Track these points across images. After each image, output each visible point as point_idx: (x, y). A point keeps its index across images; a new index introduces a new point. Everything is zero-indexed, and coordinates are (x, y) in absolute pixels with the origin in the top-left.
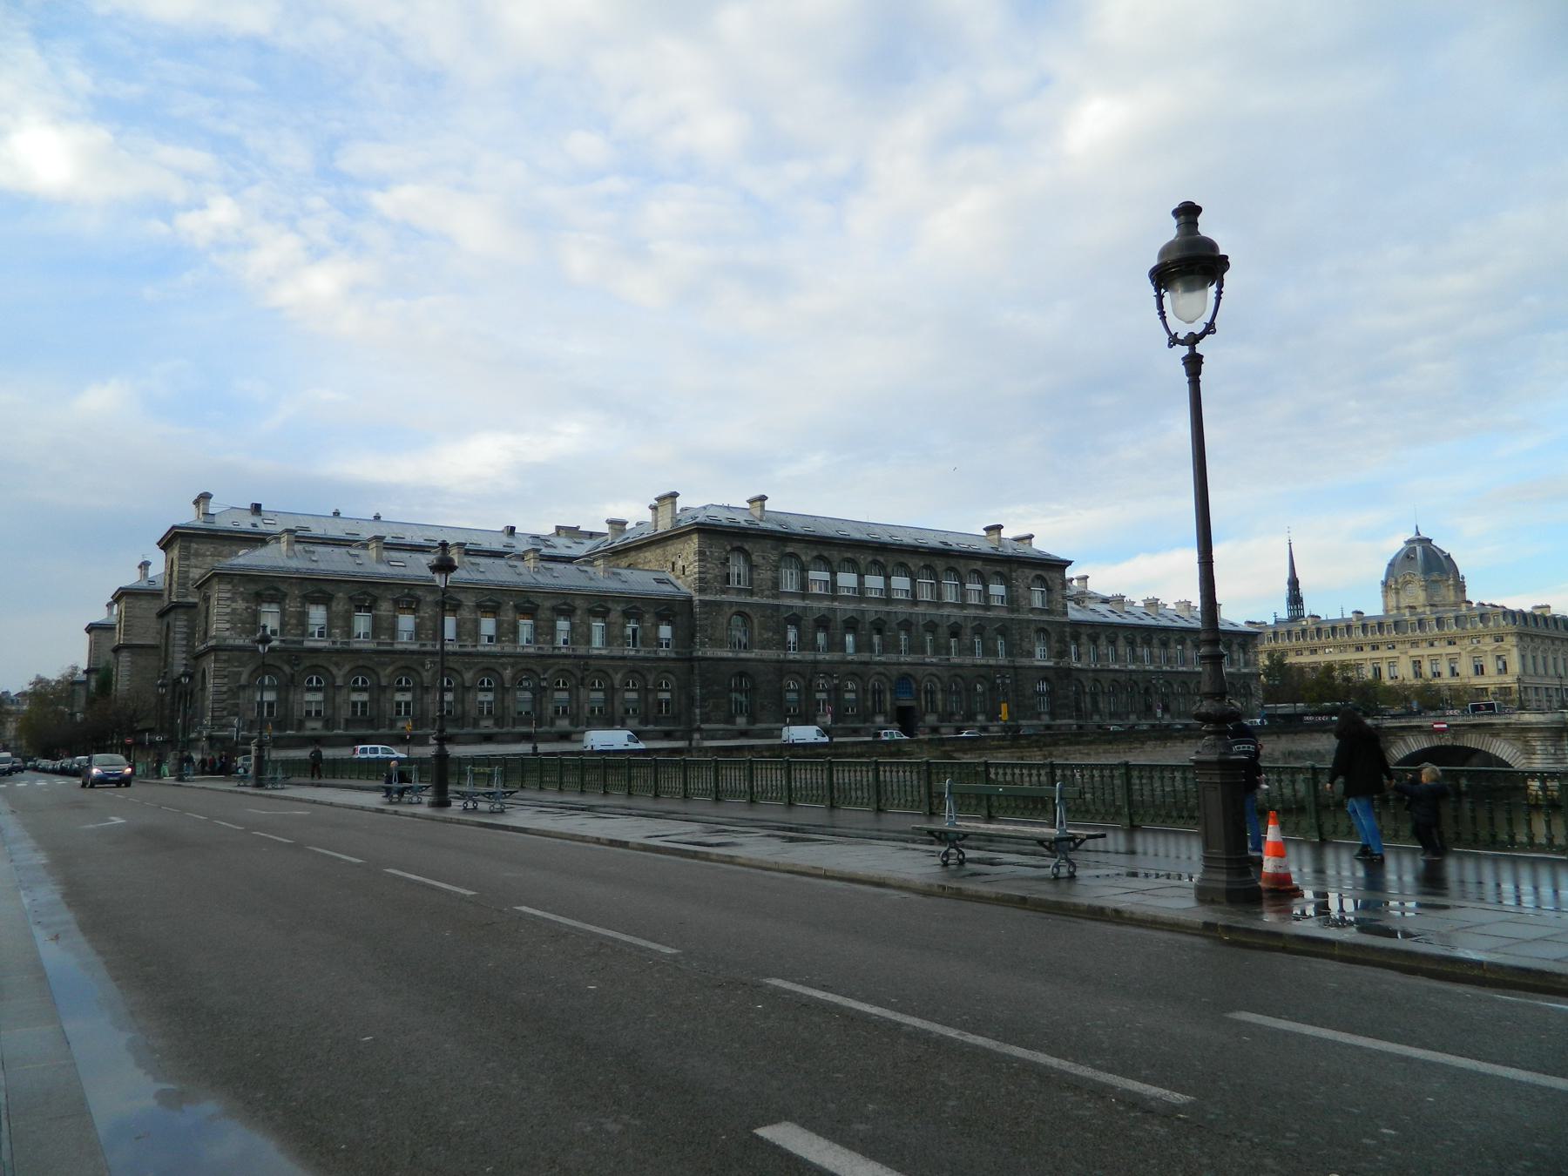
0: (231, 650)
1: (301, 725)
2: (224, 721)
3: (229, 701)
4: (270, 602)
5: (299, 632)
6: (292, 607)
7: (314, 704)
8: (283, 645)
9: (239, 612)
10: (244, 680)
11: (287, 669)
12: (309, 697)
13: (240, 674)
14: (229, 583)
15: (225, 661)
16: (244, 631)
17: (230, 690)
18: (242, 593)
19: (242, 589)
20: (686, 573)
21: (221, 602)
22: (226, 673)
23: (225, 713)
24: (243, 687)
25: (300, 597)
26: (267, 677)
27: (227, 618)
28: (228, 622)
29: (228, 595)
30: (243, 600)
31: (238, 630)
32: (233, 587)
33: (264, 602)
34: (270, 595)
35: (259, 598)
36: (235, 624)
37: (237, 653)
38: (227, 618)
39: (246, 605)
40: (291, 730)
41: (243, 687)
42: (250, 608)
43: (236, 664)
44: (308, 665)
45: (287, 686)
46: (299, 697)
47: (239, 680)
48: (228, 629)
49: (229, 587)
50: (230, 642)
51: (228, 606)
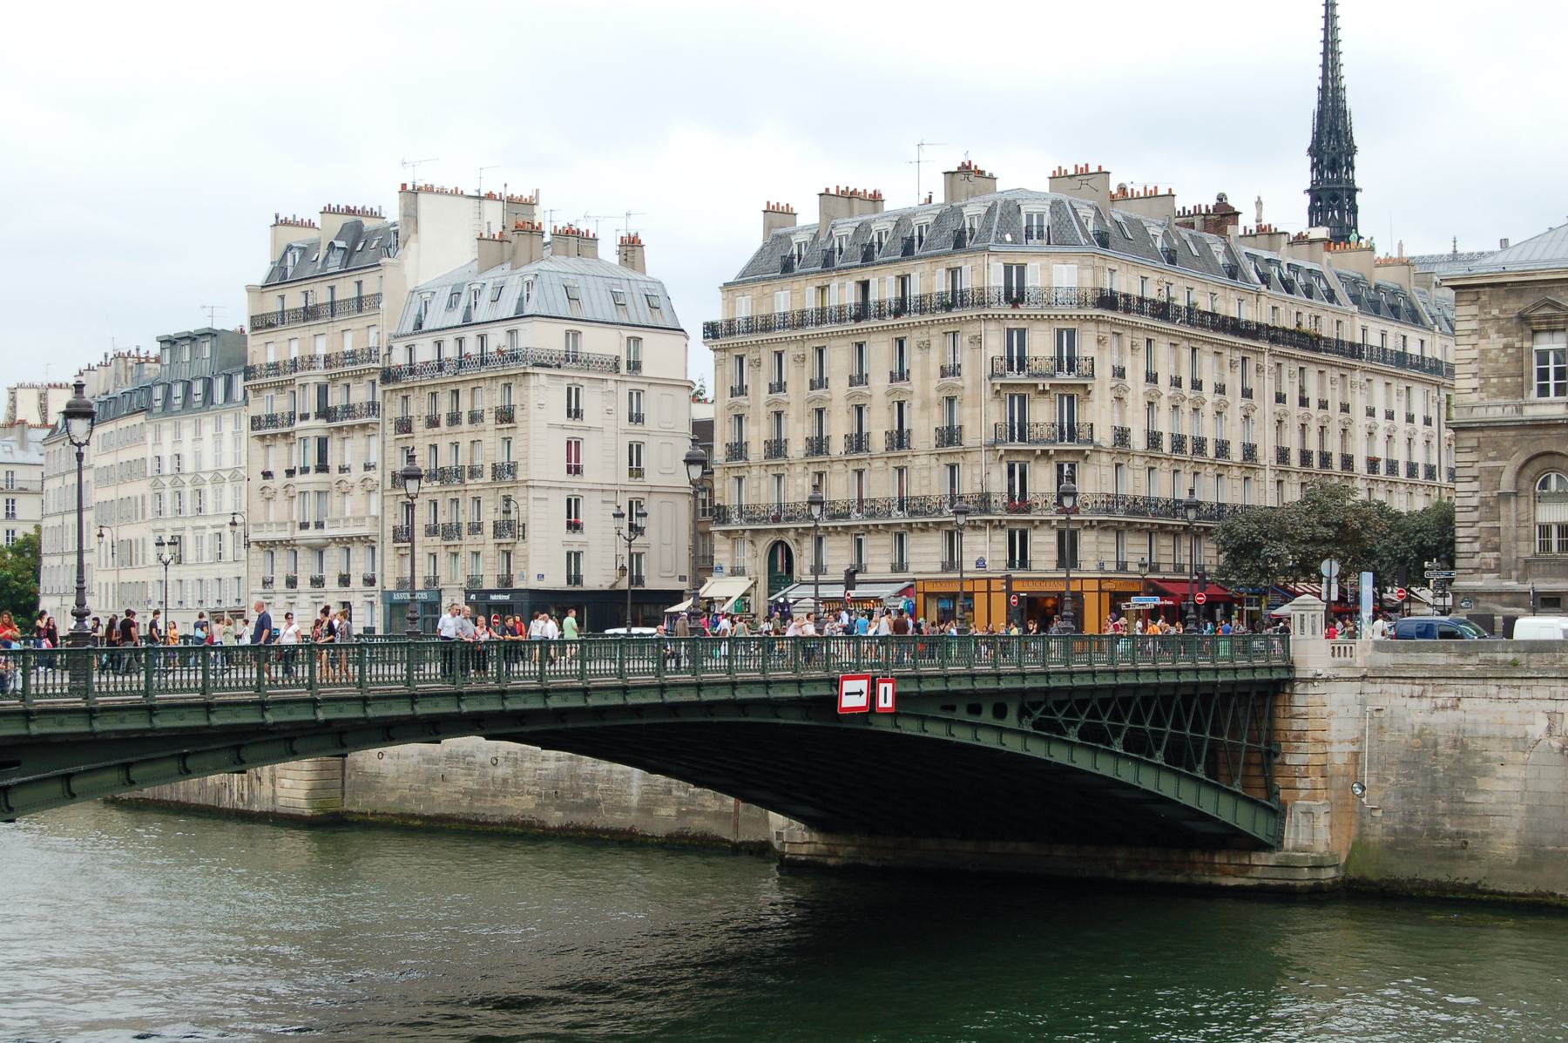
0: (1481, 429)
3: (1481, 524)
9: (1492, 355)
10: (1507, 484)
13: (1499, 472)
14: (1473, 302)
15: (1473, 449)
16: (1502, 392)
18: (1497, 319)
19: (1495, 312)
23: (1477, 546)
24: (1505, 497)
26: (1553, 477)
27: (1474, 368)
28: (1475, 375)
29: (1474, 325)
30: (1498, 332)
31: (1493, 390)
32: (1482, 307)
33: (1535, 332)
34: (1545, 317)
35: (1527, 324)
37: (1494, 434)
38: (1474, 368)
39: (1505, 340)
41: (1505, 497)
42: (1512, 346)
43: (1492, 454)
47: (1497, 487)
48: (1475, 389)
49: (1474, 310)
50: (1480, 415)
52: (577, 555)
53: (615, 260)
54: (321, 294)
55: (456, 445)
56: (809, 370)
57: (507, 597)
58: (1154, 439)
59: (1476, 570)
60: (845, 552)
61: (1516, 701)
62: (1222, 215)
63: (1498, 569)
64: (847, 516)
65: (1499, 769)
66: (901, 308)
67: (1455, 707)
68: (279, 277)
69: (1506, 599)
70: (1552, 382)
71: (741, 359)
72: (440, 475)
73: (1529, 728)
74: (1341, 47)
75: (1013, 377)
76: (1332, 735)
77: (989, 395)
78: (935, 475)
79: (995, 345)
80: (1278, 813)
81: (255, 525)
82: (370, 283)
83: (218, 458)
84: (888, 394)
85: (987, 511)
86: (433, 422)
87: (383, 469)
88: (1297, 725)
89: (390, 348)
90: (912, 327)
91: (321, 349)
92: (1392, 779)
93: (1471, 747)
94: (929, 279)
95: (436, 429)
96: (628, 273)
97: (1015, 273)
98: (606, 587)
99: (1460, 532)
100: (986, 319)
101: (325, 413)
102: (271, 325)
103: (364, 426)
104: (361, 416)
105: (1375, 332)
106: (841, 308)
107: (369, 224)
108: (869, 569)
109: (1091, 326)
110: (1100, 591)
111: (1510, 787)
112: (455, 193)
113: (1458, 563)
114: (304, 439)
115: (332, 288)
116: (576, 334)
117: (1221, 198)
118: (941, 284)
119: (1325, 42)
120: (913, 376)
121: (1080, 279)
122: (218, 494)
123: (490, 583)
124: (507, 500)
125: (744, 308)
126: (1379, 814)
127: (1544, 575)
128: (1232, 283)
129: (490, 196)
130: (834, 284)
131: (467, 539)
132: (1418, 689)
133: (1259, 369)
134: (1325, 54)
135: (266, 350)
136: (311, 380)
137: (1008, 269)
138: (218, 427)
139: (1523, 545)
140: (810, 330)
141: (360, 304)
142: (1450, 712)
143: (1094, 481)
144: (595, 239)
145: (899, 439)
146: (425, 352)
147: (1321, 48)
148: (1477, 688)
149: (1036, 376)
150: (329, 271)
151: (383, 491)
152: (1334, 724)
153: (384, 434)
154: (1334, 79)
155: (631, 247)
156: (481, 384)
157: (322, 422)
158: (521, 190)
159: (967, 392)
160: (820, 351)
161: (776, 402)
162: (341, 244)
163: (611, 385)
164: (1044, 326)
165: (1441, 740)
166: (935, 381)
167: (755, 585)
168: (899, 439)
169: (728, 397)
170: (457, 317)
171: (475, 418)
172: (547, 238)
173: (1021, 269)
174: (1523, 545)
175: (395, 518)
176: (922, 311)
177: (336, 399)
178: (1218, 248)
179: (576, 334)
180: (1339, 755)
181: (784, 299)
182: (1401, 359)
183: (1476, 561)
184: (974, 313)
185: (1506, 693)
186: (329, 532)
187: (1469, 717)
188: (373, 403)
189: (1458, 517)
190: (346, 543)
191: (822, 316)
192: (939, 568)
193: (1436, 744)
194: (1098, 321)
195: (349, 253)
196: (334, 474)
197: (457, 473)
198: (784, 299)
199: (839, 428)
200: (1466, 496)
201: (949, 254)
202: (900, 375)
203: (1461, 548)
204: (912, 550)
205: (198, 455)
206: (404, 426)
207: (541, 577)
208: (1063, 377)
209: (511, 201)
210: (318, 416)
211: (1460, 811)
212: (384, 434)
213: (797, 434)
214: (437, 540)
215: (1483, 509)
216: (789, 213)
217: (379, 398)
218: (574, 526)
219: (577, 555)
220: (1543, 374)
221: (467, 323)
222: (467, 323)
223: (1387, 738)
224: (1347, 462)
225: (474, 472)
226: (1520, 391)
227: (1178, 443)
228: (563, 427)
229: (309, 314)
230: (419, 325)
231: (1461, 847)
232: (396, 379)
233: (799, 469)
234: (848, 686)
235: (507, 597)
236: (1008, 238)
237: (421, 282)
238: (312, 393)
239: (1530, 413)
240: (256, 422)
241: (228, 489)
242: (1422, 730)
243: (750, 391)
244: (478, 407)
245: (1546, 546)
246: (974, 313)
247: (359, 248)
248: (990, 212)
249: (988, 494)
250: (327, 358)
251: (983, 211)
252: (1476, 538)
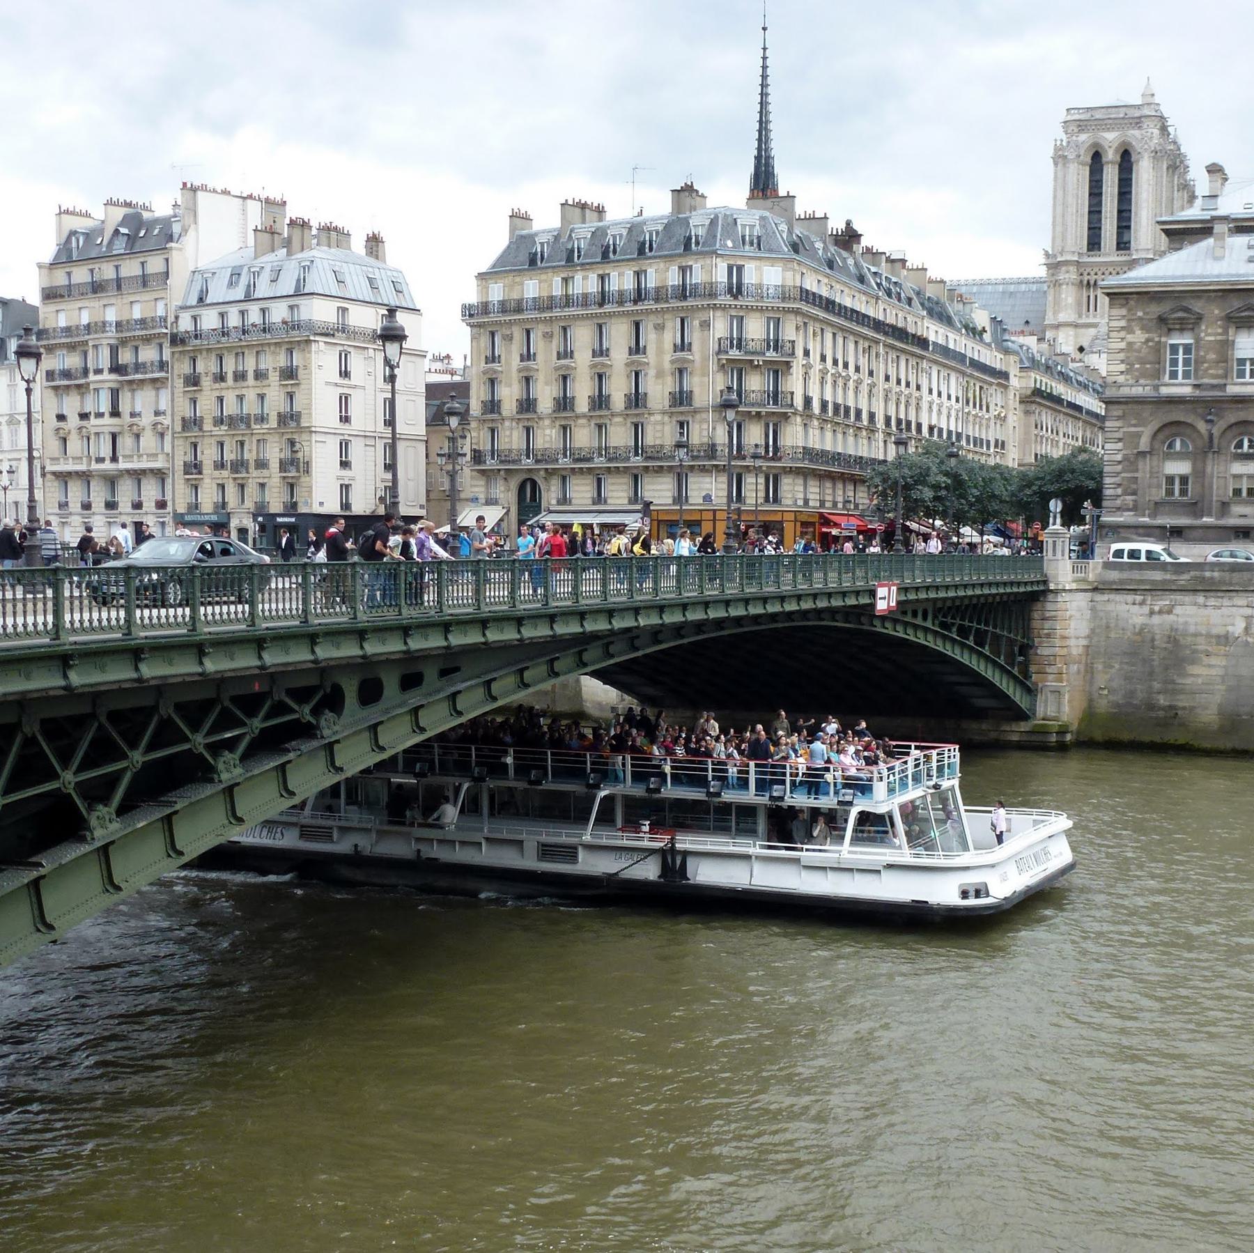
0: (1126, 403)
1: (1224, 507)
2: (1118, 502)
4: (1182, 330)
5: (1220, 372)
6: (1210, 333)
7: (1245, 479)
8: (1197, 393)
9: (1137, 346)
10: (1144, 444)
11: (1202, 426)
12: (1238, 468)
14: (1123, 306)
15: (1119, 418)
16: (1144, 375)
17: (1126, 458)
18: (1141, 319)
19: (1140, 314)
21: (1112, 335)
22: (1117, 435)
23: (1119, 491)
25: (1221, 319)
27: (1122, 356)
28: (1122, 362)
29: (1123, 323)
32: (1129, 310)
33: (1170, 330)
34: (1179, 319)
35: (1165, 324)
36: (1132, 365)
38: (1122, 356)
40: (1210, 515)
43: (1133, 422)
44: (1233, 420)
45: (1207, 449)
46: (1222, 468)
48: (1122, 373)
49: (1124, 312)
50: (1125, 391)
51: (1123, 339)
52: (347, 486)
53: (363, 252)
54: (107, 271)
55: (241, 398)
56: (556, 344)
57: (293, 520)
58: (824, 405)
59: (1119, 509)
60: (588, 488)
61: (1219, 608)
62: (849, 238)
63: (1135, 508)
64: (590, 460)
65: (1206, 660)
66: (639, 296)
67: (1170, 612)
68: (65, 257)
69: (1141, 531)
70: (1180, 368)
71: (493, 334)
72: (232, 422)
73: (1230, 629)
74: (771, 126)
75: (734, 353)
76: (1070, 632)
77: (716, 368)
78: (667, 429)
79: (720, 327)
80: (1030, 691)
81: (52, 459)
82: (155, 265)
84: (627, 365)
85: (713, 457)
86: (221, 378)
87: (173, 415)
88: (1047, 624)
89: (177, 318)
90: (648, 312)
91: (111, 316)
92: (1117, 666)
93: (1182, 642)
94: (664, 275)
95: (223, 384)
96: (372, 261)
97: (736, 271)
98: (368, 513)
99: (1107, 480)
100: (715, 307)
101: (116, 369)
102: (61, 296)
103: (154, 380)
104: (152, 372)
105: (934, 332)
106: (585, 296)
107: (146, 215)
108: (609, 501)
109: (792, 317)
110: (796, 521)
111: (1213, 672)
112: (226, 192)
113: (1105, 503)
114: (97, 390)
115: (117, 267)
116: (345, 310)
117: (848, 223)
118: (673, 278)
119: (761, 122)
120: (539, 357)
121: (784, 279)
123: (275, 507)
124: (292, 443)
125: (496, 293)
126: (1106, 692)
127: (1169, 514)
128: (860, 286)
129: (250, 197)
130: (578, 277)
131: (254, 473)
132: (1139, 598)
133: (877, 355)
134: (760, 131)
135: (59, 317)
136: (105, 342)
137: (730, 268)
139: (1154, 491)
140: (557, 313)
141: (144, 281)
142: (1166, 617)
143: (794, 436)
144: (349, 235)
145: (637, 400)
146: (210, 320)
147: (757, 126)
148: (1188, 598)
149: (753, 353)
150: (115, 252)
151: (173, 433)
152: (1073, 624)
153: (173, 387)
154: (766, 150)
155: (374, 242)
156: (266, 348)
157: (114, 377)
158: (275, 195)
159: (698, 364)
160: (565, 329)
161: (527, 369)
162: (124, 230)
163: (371, 351)
164: (758, 315)
165: (1157, 637)
166: (668, 356)
167: (507, 513)
168: (637, 400)
169: (483, 364)
170: (239, 293)
171: (260, 375)
172: (314, 232)
173: (740, 269)
174: (1154, 491)
175: (182, 456)
176: (657, 300)
177: (125, 357)
178: (851, 261)
179: (345, 310)
180: (1076, 646)
181: (532, 288)
182: (945, 351)
183: (1118, 502)
184: (705, 303)
185: (1212, 602)
186: (123, 465)
187: (1181, 620)
188: (161, 361)
189: (1106, 469)
191: (568, 301)
192: (670, 501)
193: (1153, 640)
194: (797, 312)
195: (132, 239)
196: (126, 418)
197: (245, 420)
198: (532, 288)
199: (582, 391)
200: (1109, 451)
201: (680, 255)
202: (637, 349)
203: (1107, 492)
204: (646, 487)
206: (193, 381)
207: (321, 504)
208: (771, 355)
209: (267, 201)
210: (112, 370)
211: (1172, 688)
212: (173, 387)
213: (545, 396)
214: (225, 473)
215: (1126, 463)
216: (526, 218)
217: (167, 355)
218: (345, 464)
219: (347, 486)
220: (1174, 362)
221: (248, 298)
222: (248, 298)
223: (1113, 635)
224: (919, 426)
225: (262, 419)
226: (1158, 374)
227: (837, 407)
228: (336, 384)
229: (97, 288)
230: (201, 300)
231: (1172, 716)
232: (183, 342)
233: (547, 422)
234: (882, 592)
235: (293, 520)
236: (730, 244)
237: (202, 265)
238: (105, 354)
239: (1164, 391)
242: (1142, 629)
243: (503, 358)
244: (262, 366)
245: (1170, 492)
246: (705, 303)
247: (142, 234)
248: (713, 222)
249: (714, 445)
250: (119, 325)
251: (707, 222)
252: (1119, 485)
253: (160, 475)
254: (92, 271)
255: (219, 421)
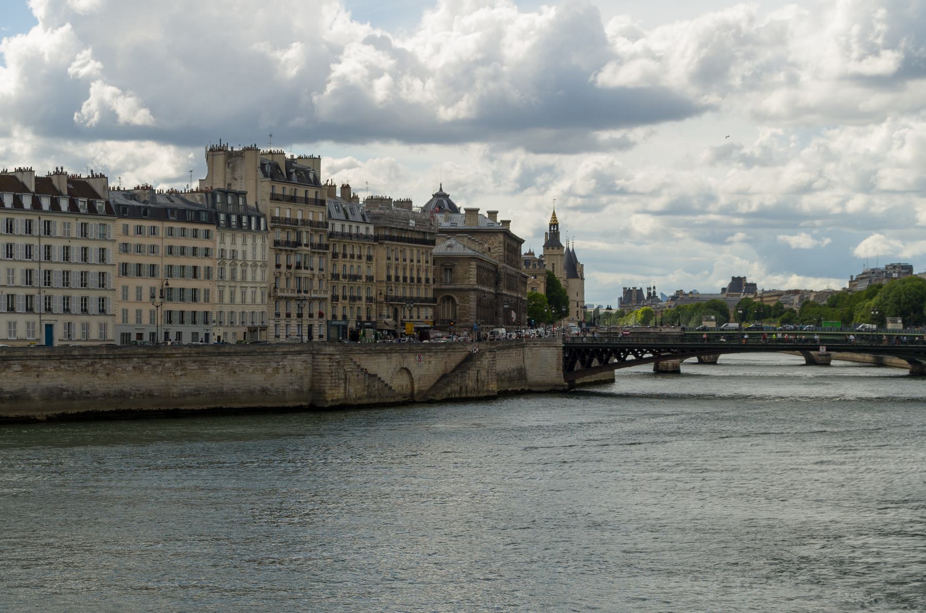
20: (492, 251)
83: (254, 256)
102: (278, 200)
104: (315, 249)
122: (254, 272)
138: (254, 241)
190: (312, 300)
205: (244, 253)
214: (347, 302)
240: (277, 243)
241: (259, 270)
253: (322, 300)
254: (284, 188)
255: (345, 277)
